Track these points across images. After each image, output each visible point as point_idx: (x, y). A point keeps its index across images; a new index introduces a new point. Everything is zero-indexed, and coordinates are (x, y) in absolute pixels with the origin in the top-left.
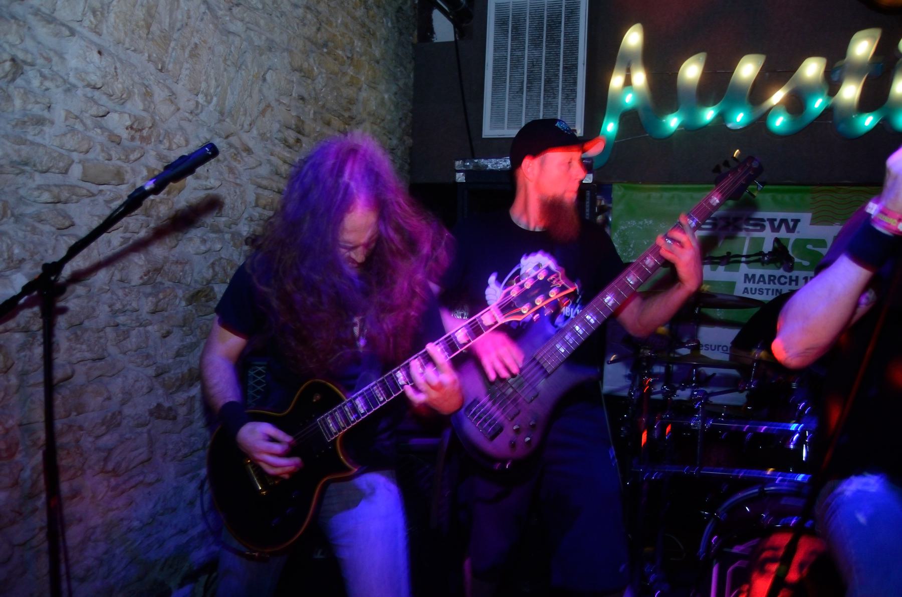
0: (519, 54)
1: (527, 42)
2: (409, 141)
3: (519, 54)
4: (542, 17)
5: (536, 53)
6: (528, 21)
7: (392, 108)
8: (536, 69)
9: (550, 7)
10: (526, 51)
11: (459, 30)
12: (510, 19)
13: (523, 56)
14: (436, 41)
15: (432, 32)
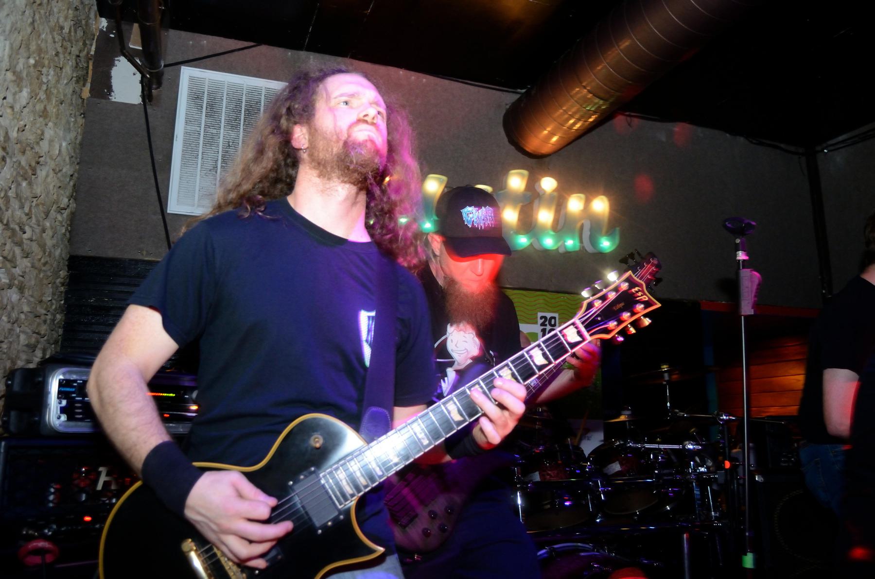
0: (214, 131)
1: (223, 121)
2: (73, 205)
3: (214, 131)
4: (240, 100)
5: (233, 134)
6: (225, 100)
7: (67, 159)
8: (231, 150)
9: (248, 93)
10: (222, 131)
11: (147, 95)
12: (206, 95)
13: (218, 134)
14: (114, 100)
15: (110, 89)
